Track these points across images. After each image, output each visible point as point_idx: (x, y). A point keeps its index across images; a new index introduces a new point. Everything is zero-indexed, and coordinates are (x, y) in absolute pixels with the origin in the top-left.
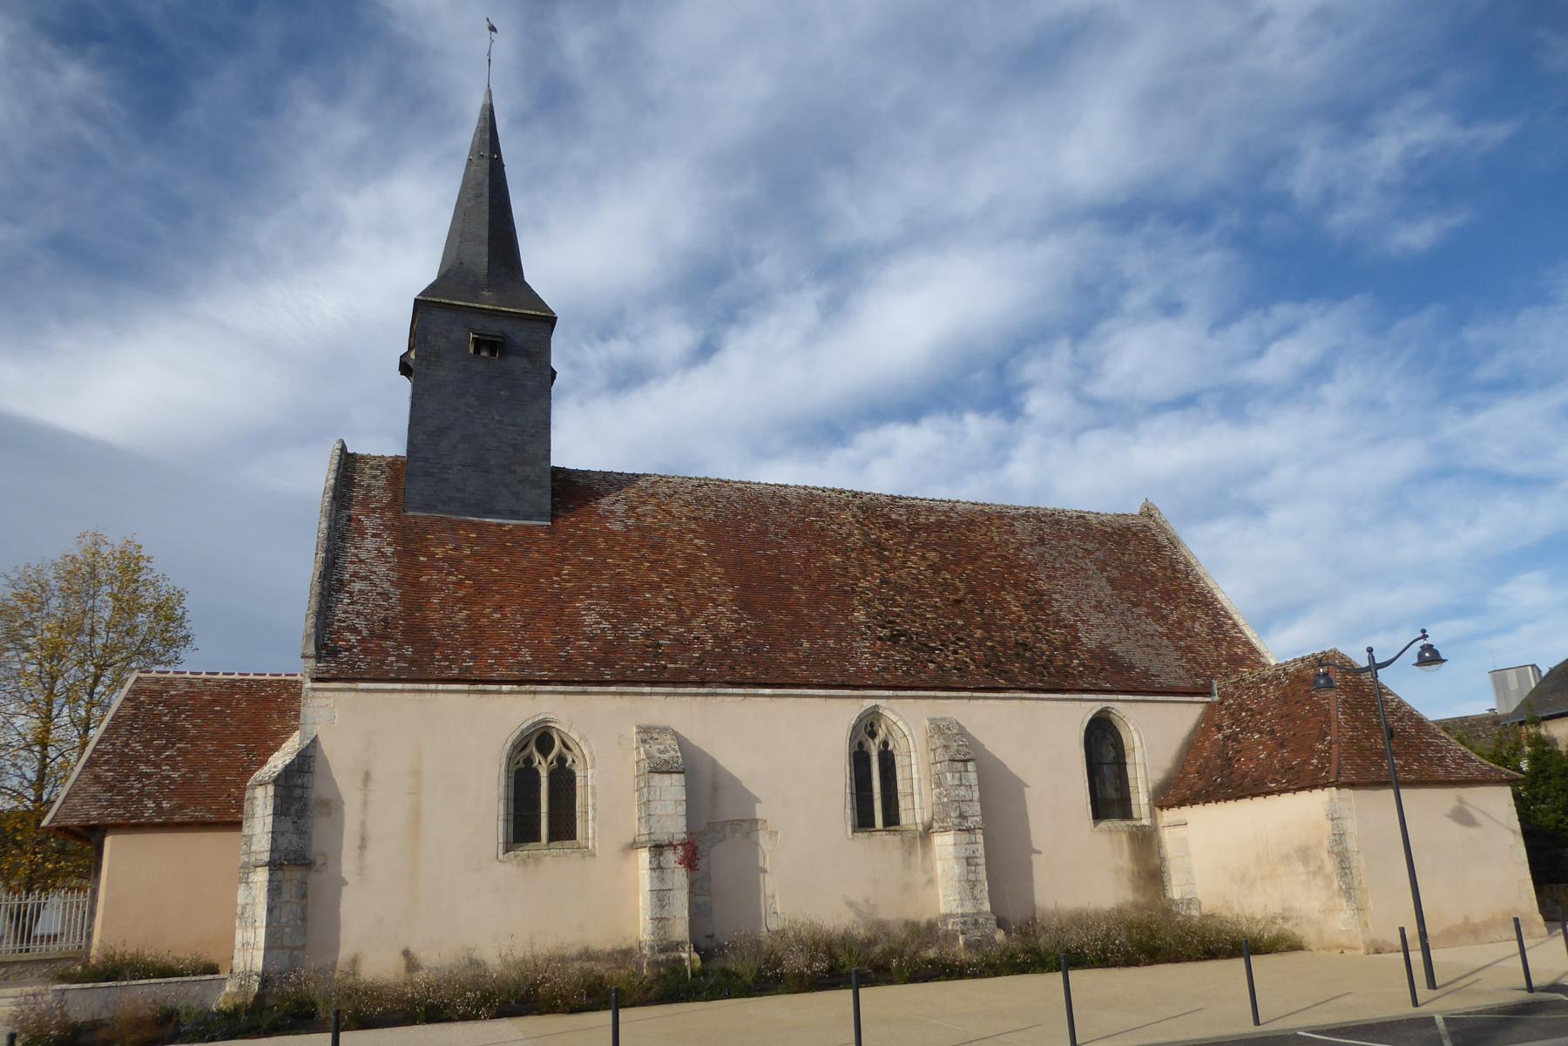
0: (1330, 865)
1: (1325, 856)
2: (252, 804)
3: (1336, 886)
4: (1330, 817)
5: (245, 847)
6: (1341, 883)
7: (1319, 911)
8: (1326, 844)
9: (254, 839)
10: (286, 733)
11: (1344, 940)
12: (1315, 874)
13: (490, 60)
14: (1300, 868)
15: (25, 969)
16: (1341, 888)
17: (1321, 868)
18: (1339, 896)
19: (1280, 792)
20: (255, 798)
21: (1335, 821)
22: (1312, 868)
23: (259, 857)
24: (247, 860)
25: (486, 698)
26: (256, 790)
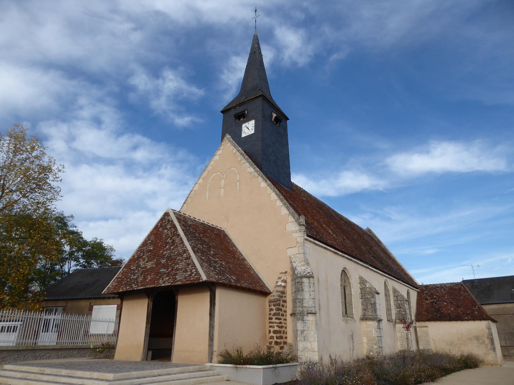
0: (487, 341)
1: (486, 339)
2: (301, 285)
3: (489, 347)
4: (488, 328)
5: (299, 304)
6: (491, 347)
7: (483, 354)
8: (486, 336)
9: (304, 301)
10: (139, 250)
11: (493, 363)
12: (481, 344)
13: (256, 21)
14: (476, 342)
15: (8, 355)
16: (491, 348)
17: (484, 342)
18: (490, 350)
19: (468, 320)
20: (303, 282)
21: (490, 330)
22: (481, 342)
23: (309, 309)
24: (301, 310)
25: (336, 256)
26: (303, 279)
